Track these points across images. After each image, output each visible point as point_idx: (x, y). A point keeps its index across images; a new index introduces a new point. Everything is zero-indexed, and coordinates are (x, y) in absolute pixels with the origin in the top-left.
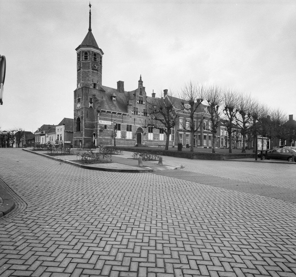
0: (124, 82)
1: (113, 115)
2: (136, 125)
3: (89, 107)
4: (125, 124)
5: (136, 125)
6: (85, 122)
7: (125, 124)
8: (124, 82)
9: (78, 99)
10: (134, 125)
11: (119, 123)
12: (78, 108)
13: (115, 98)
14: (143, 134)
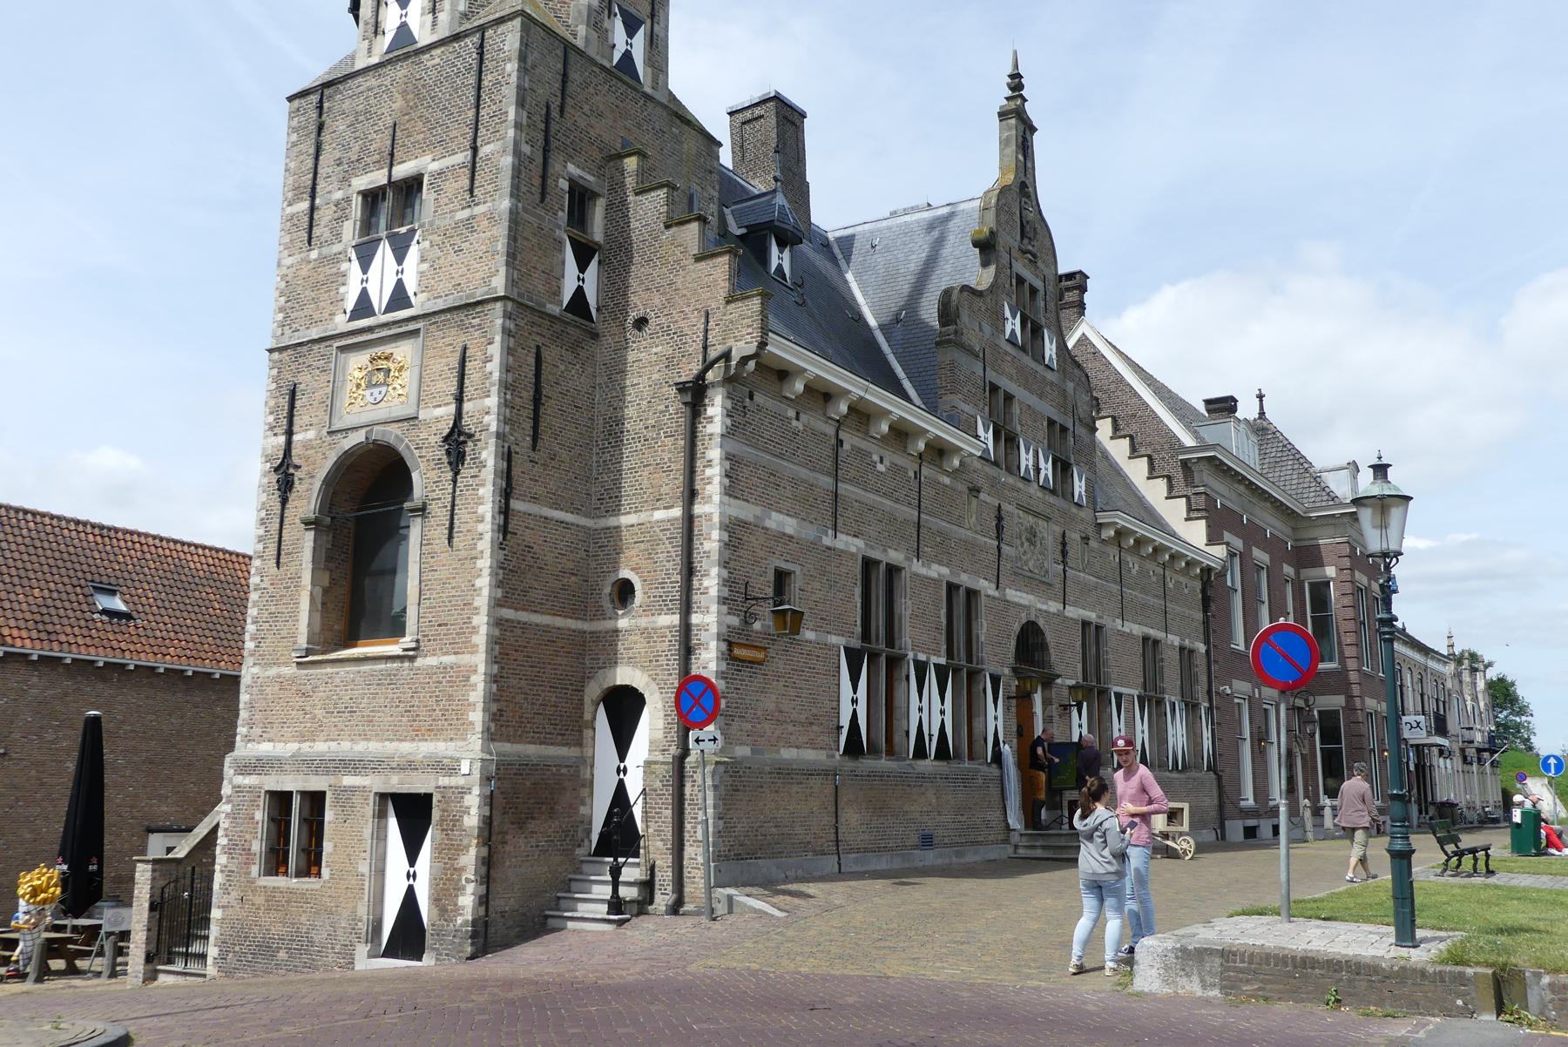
0: (803, 115)
1: (850, 440)
2: (1012, 595)
3: (557, 293)
4: (937, 571)
5: (1012, 595)
6: (505, 511)
7: (937, 571)
8: (803, 115)
9: (372, 198)
10: (992, 592)
11: (895, 556)
12: (363, 306)
13: (786, 254)
14: (1046, 703)
